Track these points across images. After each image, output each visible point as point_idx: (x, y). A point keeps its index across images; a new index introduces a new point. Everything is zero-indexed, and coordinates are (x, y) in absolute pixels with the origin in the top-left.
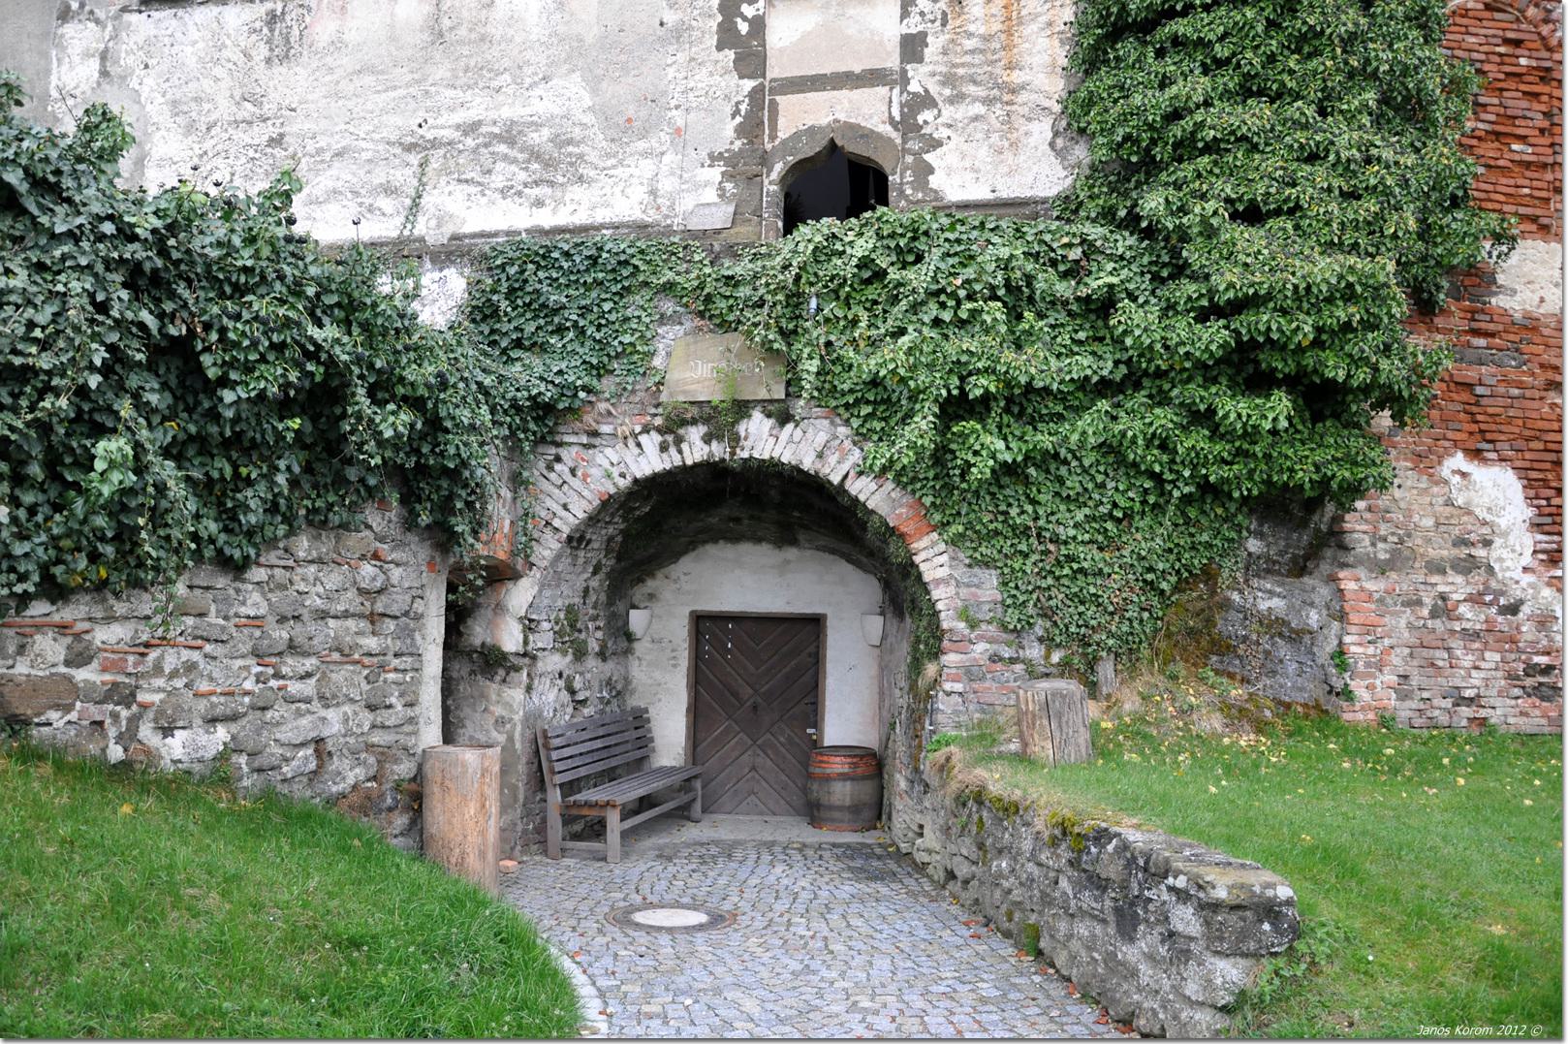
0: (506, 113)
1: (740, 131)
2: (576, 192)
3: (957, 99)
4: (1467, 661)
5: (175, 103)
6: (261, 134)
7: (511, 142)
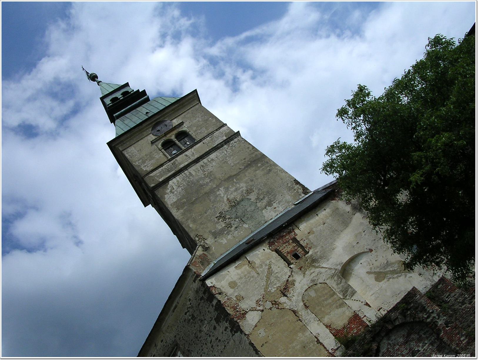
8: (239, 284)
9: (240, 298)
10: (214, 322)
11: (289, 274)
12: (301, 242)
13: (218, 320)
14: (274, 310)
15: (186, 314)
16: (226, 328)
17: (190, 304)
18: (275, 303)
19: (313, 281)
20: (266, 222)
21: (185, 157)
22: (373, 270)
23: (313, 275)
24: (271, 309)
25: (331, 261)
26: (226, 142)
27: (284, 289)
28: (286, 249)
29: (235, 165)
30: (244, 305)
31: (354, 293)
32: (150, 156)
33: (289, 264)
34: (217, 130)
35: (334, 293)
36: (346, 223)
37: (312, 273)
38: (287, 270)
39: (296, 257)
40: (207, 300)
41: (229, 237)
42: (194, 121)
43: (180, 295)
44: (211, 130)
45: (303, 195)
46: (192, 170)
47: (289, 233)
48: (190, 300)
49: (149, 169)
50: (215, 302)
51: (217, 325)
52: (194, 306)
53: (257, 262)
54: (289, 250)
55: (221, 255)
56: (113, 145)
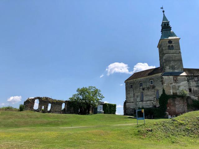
9: (165, 81)
26: (178, 53)
30: (165, 82)
36: (185, 81)
37: (176, 84)
39: (175, 81)
44: (178, 49)
46: (170, 54)
53: (170, 78)
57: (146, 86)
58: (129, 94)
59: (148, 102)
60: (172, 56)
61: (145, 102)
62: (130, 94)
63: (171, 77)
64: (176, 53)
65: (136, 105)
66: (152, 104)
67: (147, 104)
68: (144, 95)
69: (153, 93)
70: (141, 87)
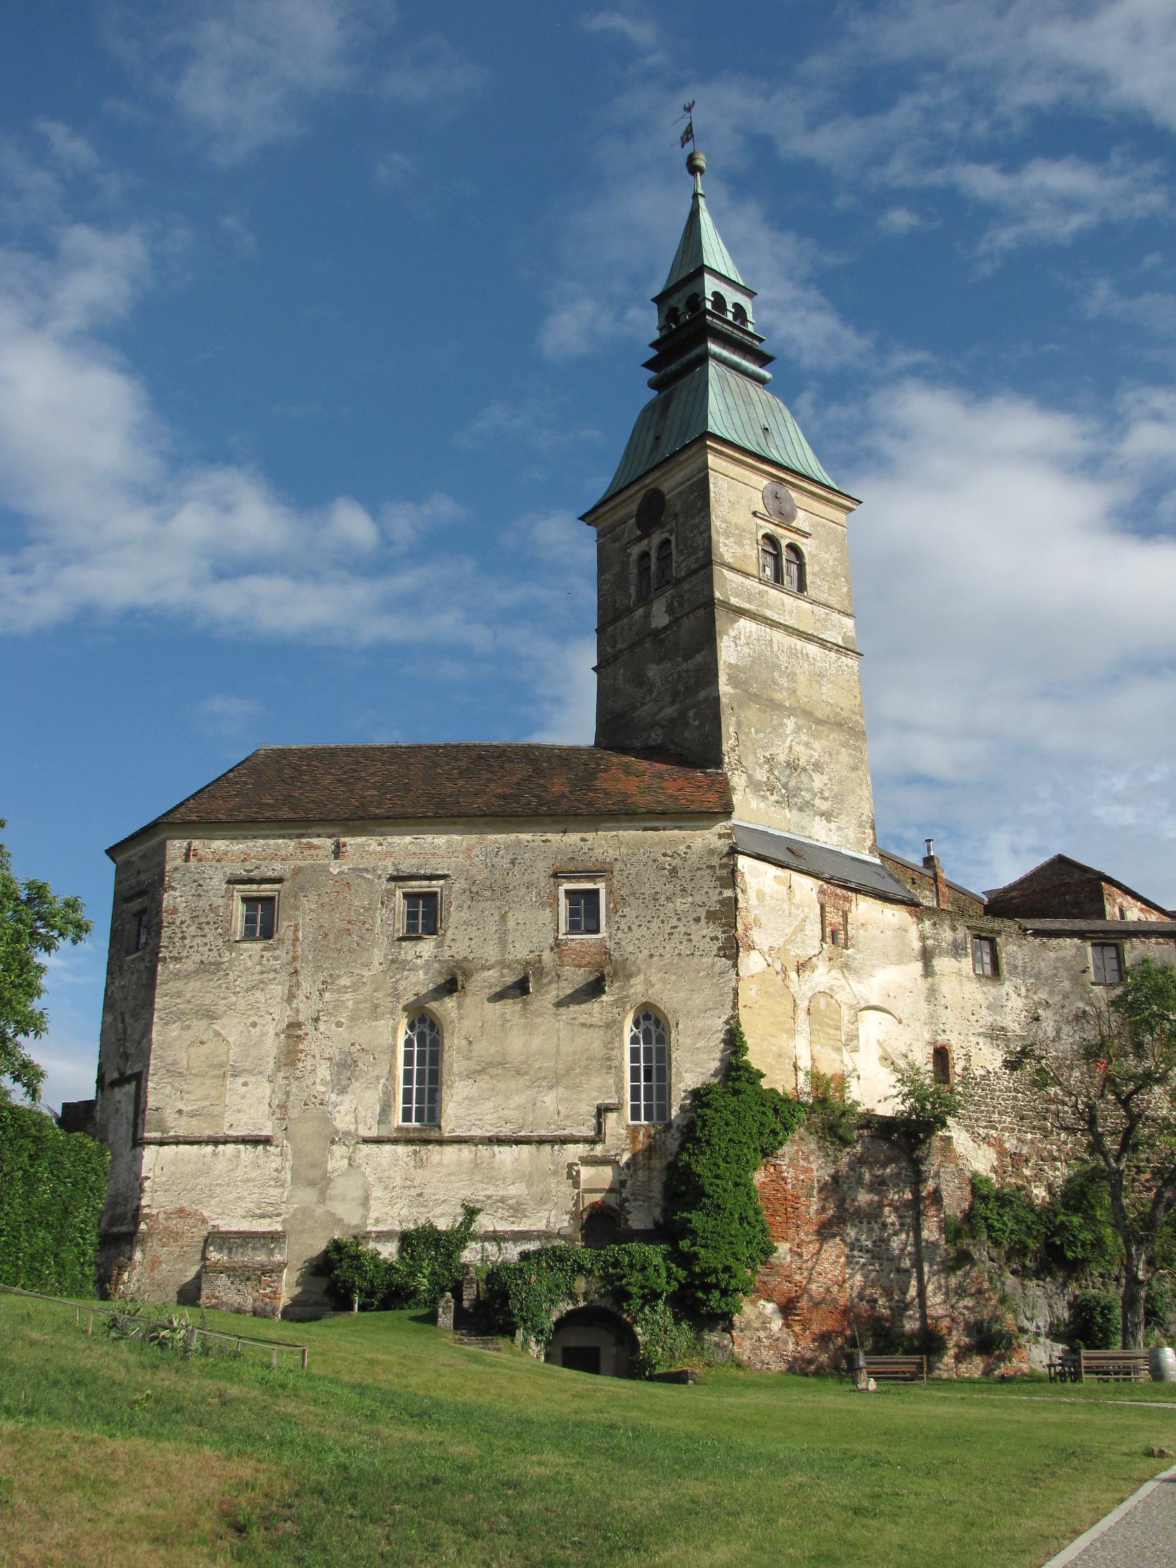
0: (500, 1193)
1: (575, 1205)
2: (525, 1220)
3: (635, 1200)
4: (765, 1353)
5: (380, 1178)
6: (413, 1192)
7: (503, 1203)
8: (766, 903)
9: (757, 923)
10: (702, 913)
11: (817, 953)
12: (849, 927)
13: (711, 916)
14: (780, 977)
15: (665, 855)
16: (717, 938)
17: (685, 853)
18: (785, 970)
19: (831, 989)
20: (810, 837)
21: (779, 603)
22: (885, 1045)
23: (835, 982)
24: (777, 973)
25: (860, 986)
27: (802, 964)
28: (834, 918)
29: (828, 704)
30: (757, 936)
31: (855, 1050)
32: (739, 534)
33: (823, 939)
34: (840, 612)
35: (838, 1028)
36: (901, 959)
38: (817, 943)
40: (718, 879)
41: (762, 805)
42: (823, 555)
43: (677, 825)
44: (833, 601)
45: (867, 852)
47: (846, 899)
48: (689, 847)
49: (728, 558)
50: (728, 893)
51: (703, 921)
52: (690, 862)
54: (833, 921)
55: (741, 820)
56: (708, 443)
57: (503, 942)
58: (211, 1016)
59: (506, 1154)
60: (793, 653)
61: (466, 1152)
62: (232, 1029)
63: (806, 887)
64: (823, 643)
65: (321, 1183)
66: (566, 1188)
67: (490, 1180)
68: (454, 1060)
69: (595, 1042)
70: (427, 947)
